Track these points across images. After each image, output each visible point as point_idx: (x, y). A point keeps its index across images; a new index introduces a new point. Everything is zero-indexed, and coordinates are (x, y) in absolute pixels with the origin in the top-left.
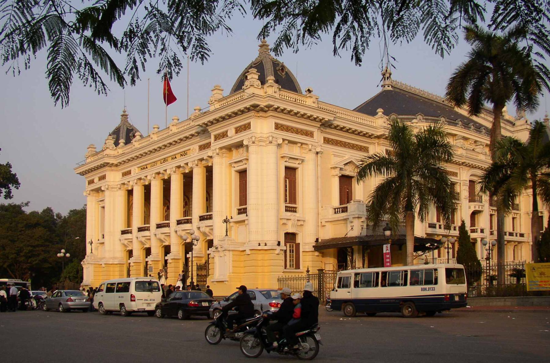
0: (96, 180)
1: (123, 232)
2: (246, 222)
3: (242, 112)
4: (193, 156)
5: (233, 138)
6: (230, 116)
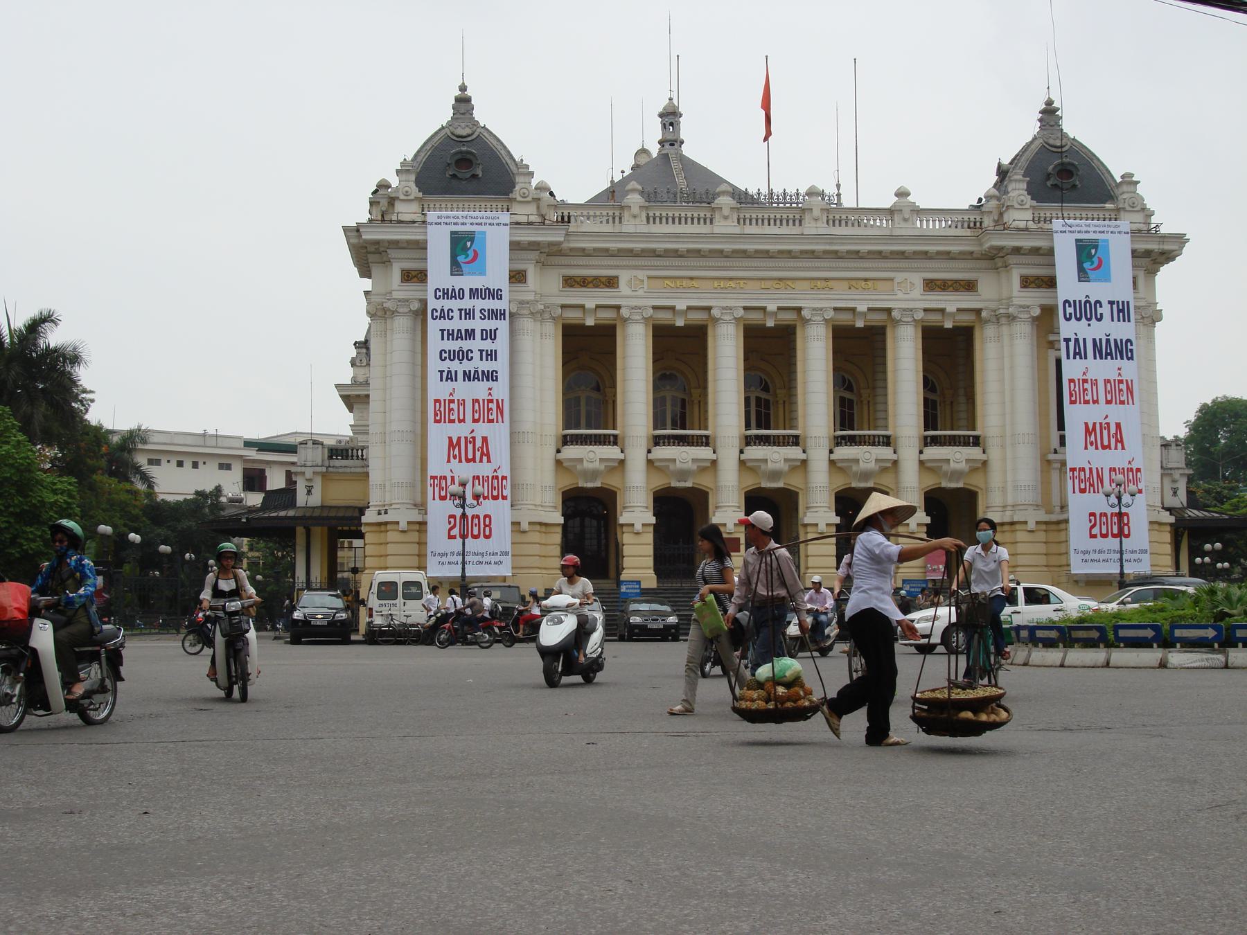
1: (566, 441)
4: (900, 295)
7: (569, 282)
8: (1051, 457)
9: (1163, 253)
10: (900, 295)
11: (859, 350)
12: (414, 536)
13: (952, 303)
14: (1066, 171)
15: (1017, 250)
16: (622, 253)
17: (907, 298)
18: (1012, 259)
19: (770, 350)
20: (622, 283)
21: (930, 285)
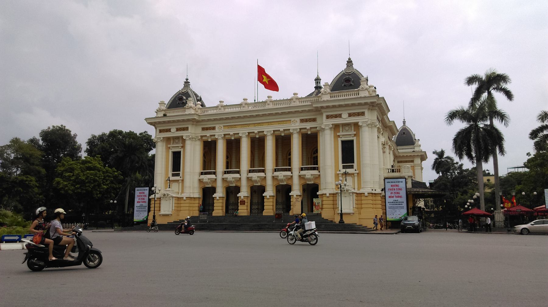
0: (173, 130)
1: (202, 174)
2: (356, 175)
3: (360, 104)
4: (293, 125)
5: (345, 119)
6: (347, 105)
7: (203, 129)
8: (338, 172)
9: (372, 103)
10: (293, 125)
11: (283, 142)
12: (331, 198)
13: (308, 125)
14: (348, 80)
15: (322, 107)
16: (215, 120)
17: (295, 126)
18: (323, 110)
19: (258, 144)
20: (217, 128)
21: (302, 121)
